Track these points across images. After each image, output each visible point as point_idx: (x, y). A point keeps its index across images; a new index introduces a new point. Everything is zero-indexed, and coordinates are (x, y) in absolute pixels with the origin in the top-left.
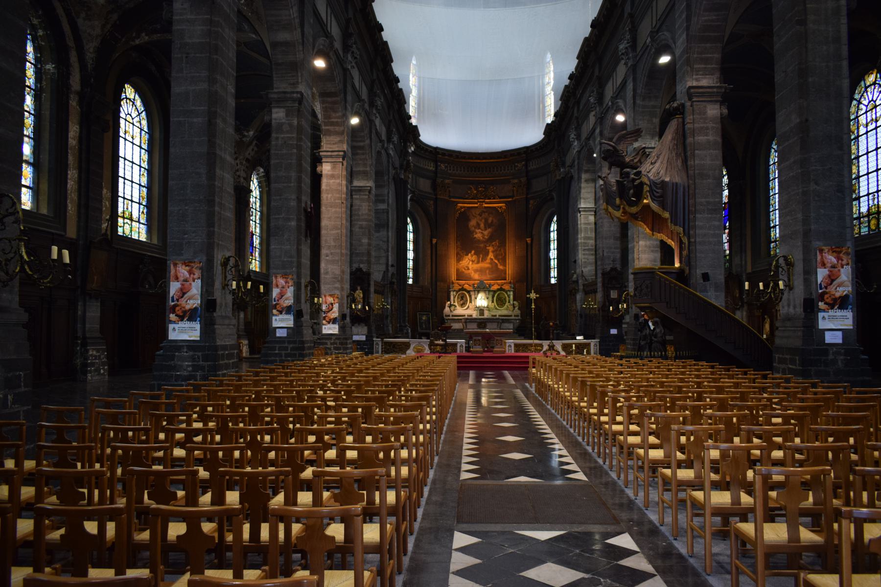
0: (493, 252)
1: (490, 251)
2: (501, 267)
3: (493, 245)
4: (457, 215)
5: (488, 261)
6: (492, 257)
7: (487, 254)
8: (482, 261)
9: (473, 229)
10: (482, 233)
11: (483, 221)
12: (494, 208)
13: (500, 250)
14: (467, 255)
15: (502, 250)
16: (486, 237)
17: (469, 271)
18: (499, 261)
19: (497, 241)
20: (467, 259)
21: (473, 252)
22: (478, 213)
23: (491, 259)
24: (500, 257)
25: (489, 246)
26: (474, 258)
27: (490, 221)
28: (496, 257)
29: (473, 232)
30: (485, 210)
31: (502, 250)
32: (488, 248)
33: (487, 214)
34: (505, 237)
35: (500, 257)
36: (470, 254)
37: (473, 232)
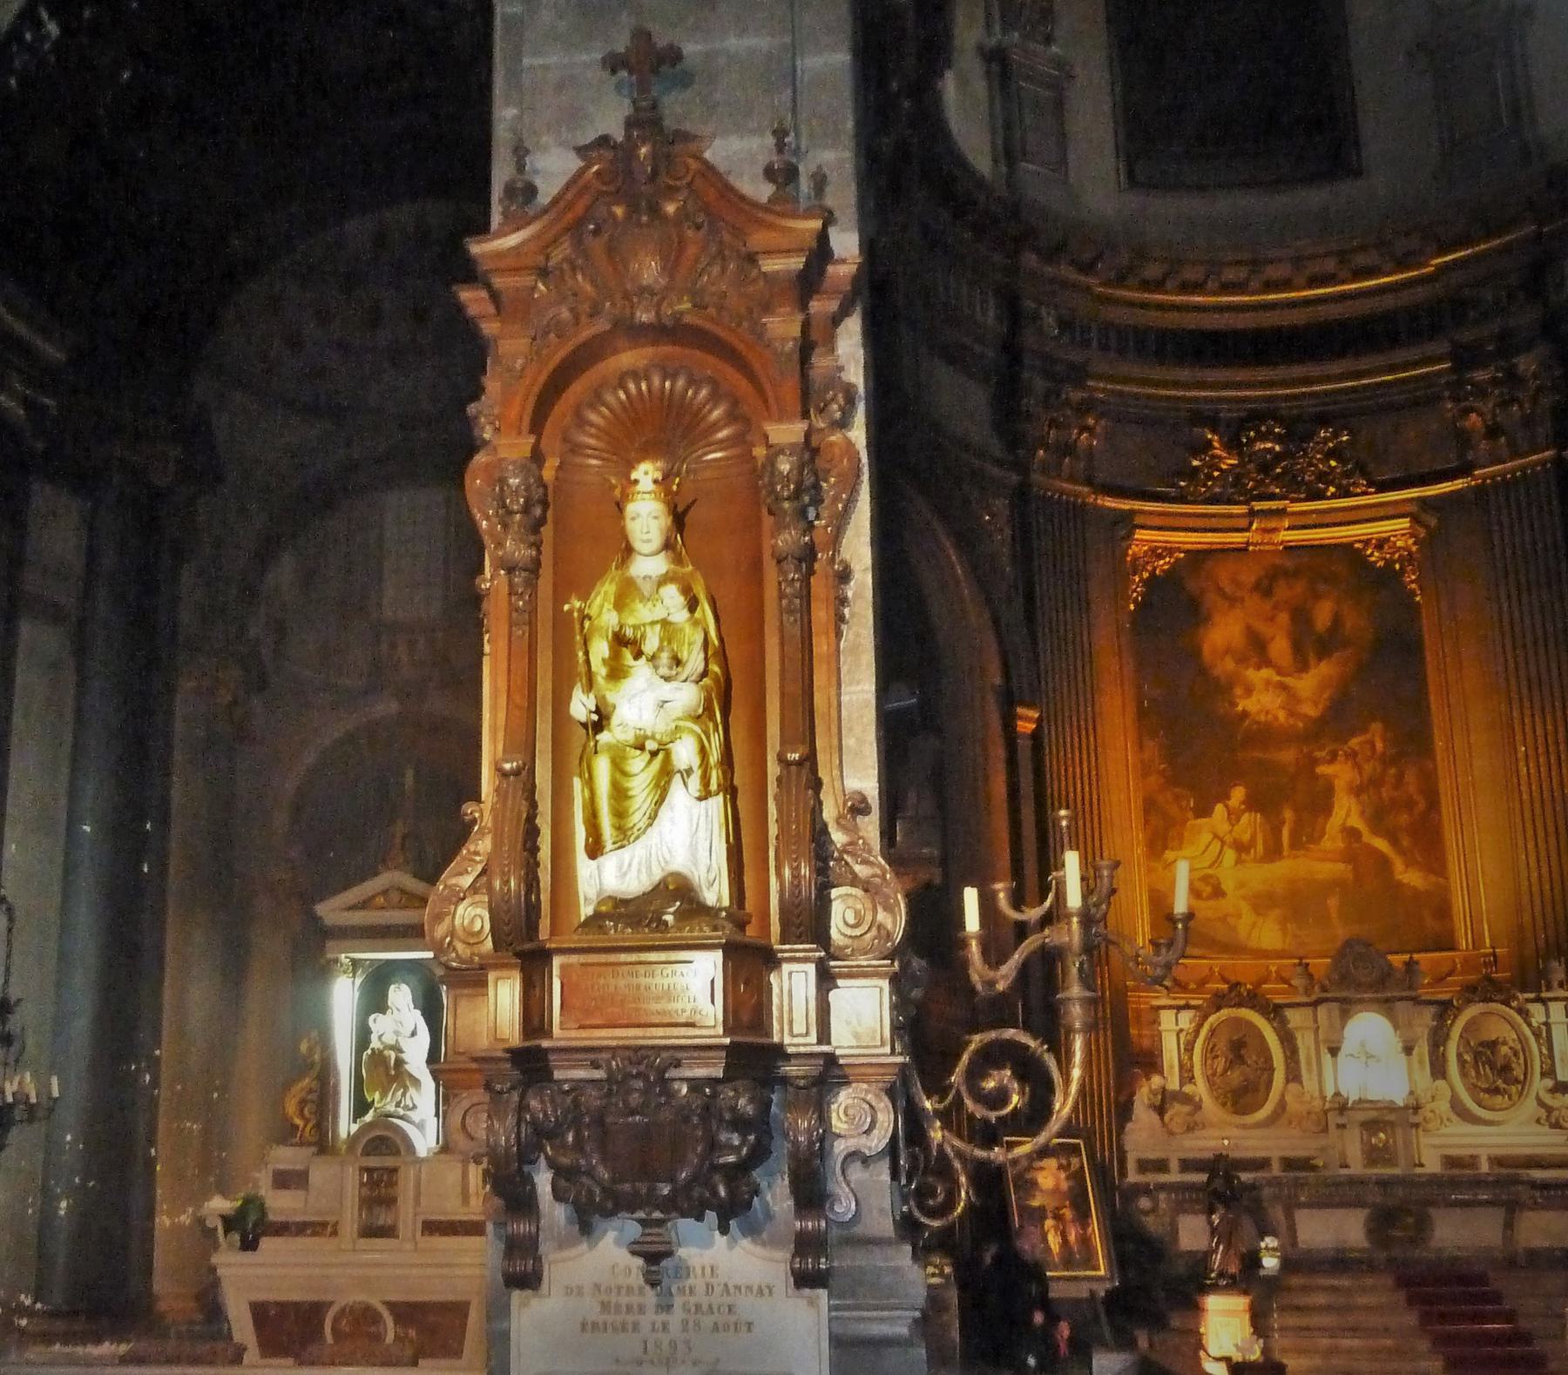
0: (1357, 791)
1: (1340, 785)
2: (1411, 877)
3: (1352, 755)
4: (1136, 589)
5: (1332, 840)
6: (1356, 822)
7: (1321, 804)
8: (1295, 844)
9: (1229, 664)
10: (1283, 687)
11: (1284, 618)
12: (1346, 550)
13: (1400, 777)
14: (1204, 811)
15: (1411, 777)
16: (1310, 710)
17: (1225, 905)
18: (1394, 842)
19: (1376, 727)
20: (1206, 837)
21: (1238, 794)
22: (1249, 576)
23: (1352, 834)
24: (1404, 819)
25: (1333, 758)
26: (1249, 824)
27: (1323, 615)
28: (1377, 820)
29: (1223, 689)
30: (1289, 563)
31: (1411, 777)
32: (1322, 769)
33: (1300, 587)
34: (1418, 705)
35: (1404, 819)
36: (1219, 809)
37: (1230, 687)
